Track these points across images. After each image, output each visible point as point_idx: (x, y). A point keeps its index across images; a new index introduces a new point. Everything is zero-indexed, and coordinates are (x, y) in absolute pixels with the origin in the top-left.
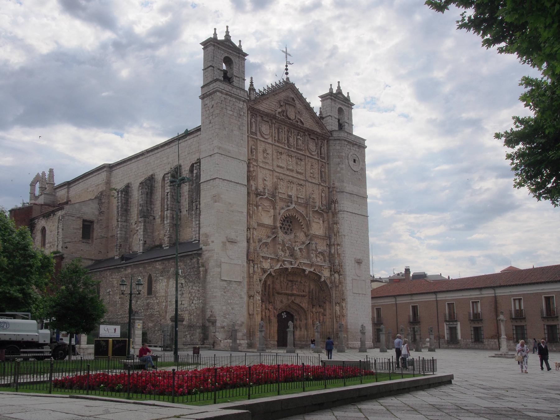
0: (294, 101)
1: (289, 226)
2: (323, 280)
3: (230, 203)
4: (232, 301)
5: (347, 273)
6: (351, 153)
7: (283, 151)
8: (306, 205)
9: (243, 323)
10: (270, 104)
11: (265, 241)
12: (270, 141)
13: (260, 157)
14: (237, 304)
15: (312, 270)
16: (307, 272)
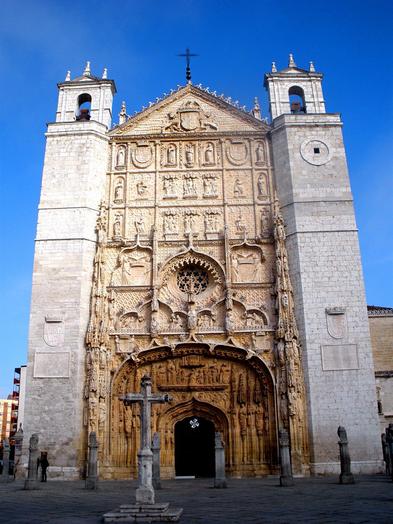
0: (198, 105)
1: (200, 280)
2: (249, 357)
3: (54, 269)
4: (51, 407)
5: (307, 337)
6: (307, 142)
7: (173, 175)
8: (222, 242)
9: (71, 440)
10: (153, 123)
11: (129, 312)
12: (152, 168)
13: (132, 194)
14: (59, 412)
15: (224, 343)
16: (212, 349)
